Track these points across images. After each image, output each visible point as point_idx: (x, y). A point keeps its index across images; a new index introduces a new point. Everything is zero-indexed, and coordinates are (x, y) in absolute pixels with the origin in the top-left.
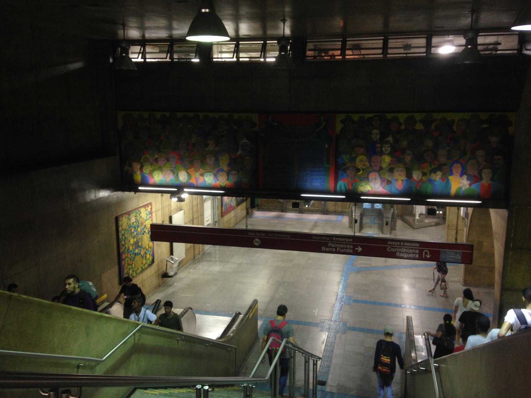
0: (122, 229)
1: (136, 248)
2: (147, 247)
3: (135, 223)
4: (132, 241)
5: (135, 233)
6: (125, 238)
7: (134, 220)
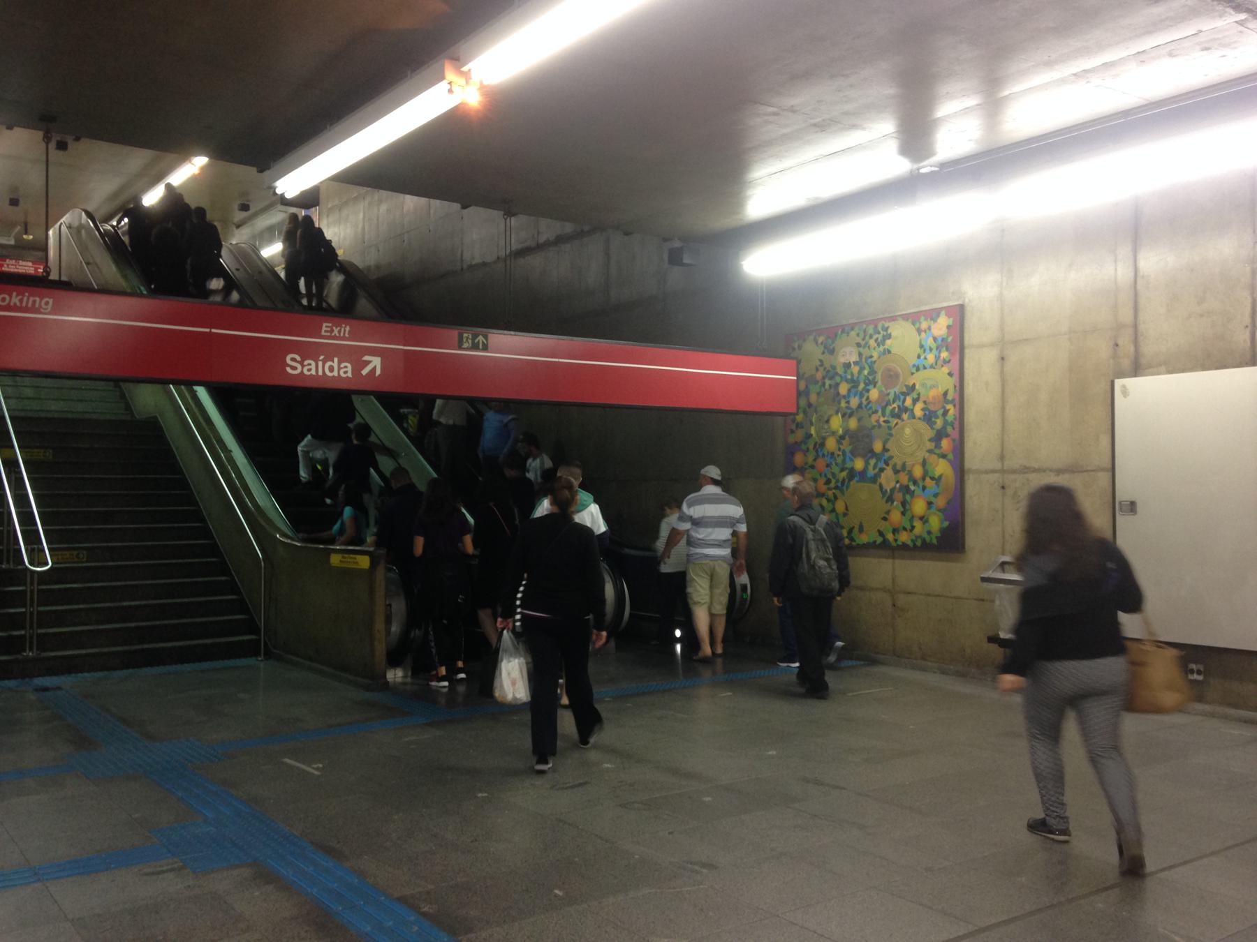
1: (854, 454)
2: (918, 472)
3: (855, 369)
5: (854, 402)
6: (810, 405)
7: (854, 358)
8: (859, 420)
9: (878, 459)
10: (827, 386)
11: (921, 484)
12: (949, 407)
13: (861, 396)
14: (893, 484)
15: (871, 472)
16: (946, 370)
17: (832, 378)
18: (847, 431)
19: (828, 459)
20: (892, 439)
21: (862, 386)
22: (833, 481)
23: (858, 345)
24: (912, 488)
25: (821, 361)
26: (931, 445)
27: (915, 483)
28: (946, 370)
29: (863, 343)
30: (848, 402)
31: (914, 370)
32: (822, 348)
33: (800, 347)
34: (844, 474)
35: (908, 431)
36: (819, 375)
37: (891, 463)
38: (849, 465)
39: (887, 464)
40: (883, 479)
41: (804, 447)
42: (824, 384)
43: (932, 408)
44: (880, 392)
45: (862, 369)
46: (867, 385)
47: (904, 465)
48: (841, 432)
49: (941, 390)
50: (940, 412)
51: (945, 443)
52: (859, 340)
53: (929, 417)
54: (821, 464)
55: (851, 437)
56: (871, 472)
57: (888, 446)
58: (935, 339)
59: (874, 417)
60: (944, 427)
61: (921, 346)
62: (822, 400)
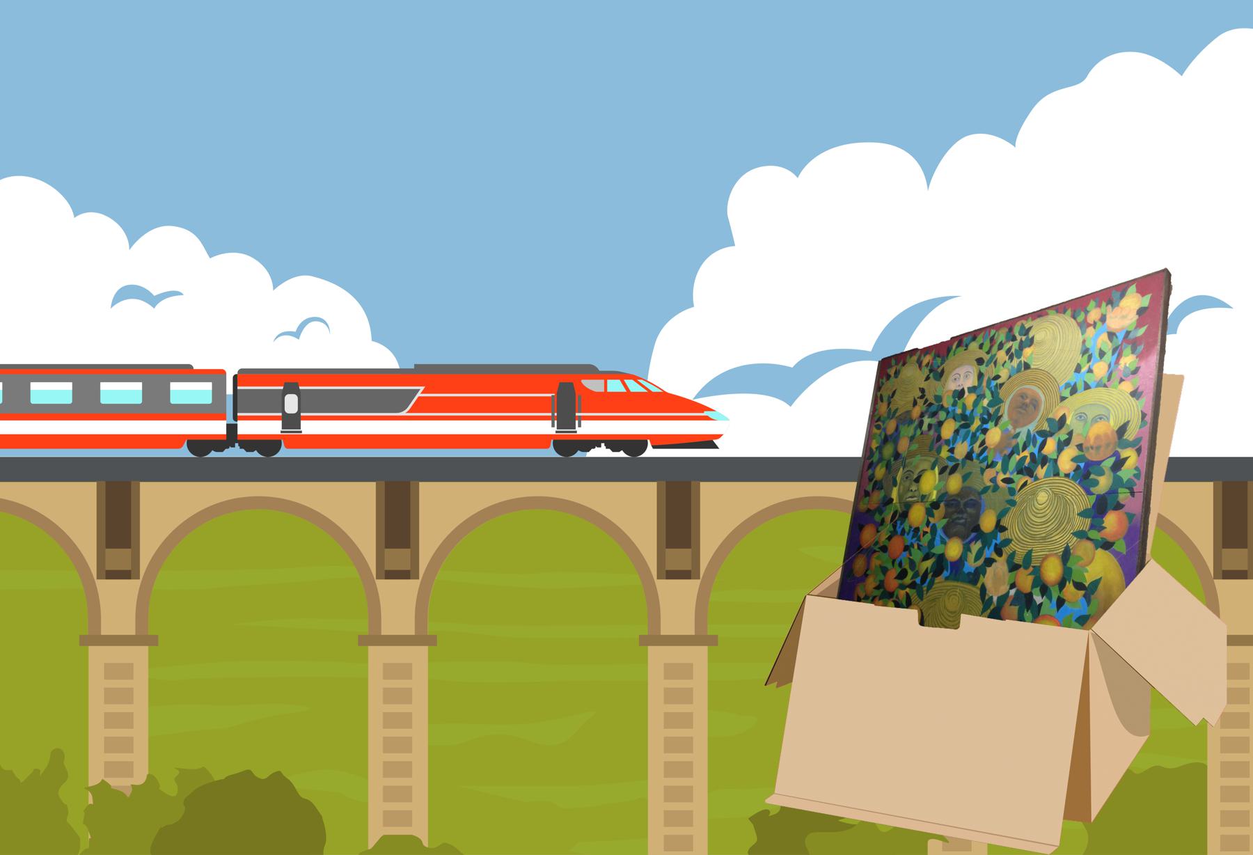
0: (891, 415)
1: (949, 532)
3: (970, 399)
4: (930, 484)
5: (961, 449)
6: (897, 455)
7: (972, 381)
8: (965, 478)
9: (986, 544)
10: (925, 427)
11: (1055, 594)
12: (1130, 454)
13: (974, 437)
14: (1004, 589)
15: (971, 565)
16: (1127, 387)
17: (934, 414)
18: (943, 496)
19: (908, 539)
20: (1013, 509)
21: (977, 423)
22: (910, 574)
23: (980, 361)
24: (1038, 599)
25: (922, 390)
26: (1083, 524)
27: (1045, 590)
28: (1127, 387)
29: (986, 357)
30: (952, 451)
31: (1066, 393)
32: (926, 371)
33: (897, 373)
34: (928, 564)
35: (1042, 497)
36: (916, 412)
37: (1007, 551)
38: (938, 550)
39: (999, 552)
40: (988, 579)
41: (878, 518)
42: (921, 423)
43: (1092, 456)
44: (1005, 432)
45: (982, 396)
46: (984, 421)
47: (1028, 556)
48: (934, 497)
49: (1114, 424)
50: (1109, 463)
51: (1111, 521)
52: (982, 354)
53: (1085, 473)
54: (897, 544)
55: (947, 505)
56: (971, 565)
57: (1004, 523)
58: (1111, 335)
59: (990, 473)
60: (1113, 492)
61: (1085, 351)
62: (915, 447)
